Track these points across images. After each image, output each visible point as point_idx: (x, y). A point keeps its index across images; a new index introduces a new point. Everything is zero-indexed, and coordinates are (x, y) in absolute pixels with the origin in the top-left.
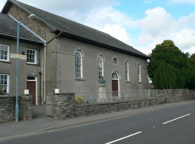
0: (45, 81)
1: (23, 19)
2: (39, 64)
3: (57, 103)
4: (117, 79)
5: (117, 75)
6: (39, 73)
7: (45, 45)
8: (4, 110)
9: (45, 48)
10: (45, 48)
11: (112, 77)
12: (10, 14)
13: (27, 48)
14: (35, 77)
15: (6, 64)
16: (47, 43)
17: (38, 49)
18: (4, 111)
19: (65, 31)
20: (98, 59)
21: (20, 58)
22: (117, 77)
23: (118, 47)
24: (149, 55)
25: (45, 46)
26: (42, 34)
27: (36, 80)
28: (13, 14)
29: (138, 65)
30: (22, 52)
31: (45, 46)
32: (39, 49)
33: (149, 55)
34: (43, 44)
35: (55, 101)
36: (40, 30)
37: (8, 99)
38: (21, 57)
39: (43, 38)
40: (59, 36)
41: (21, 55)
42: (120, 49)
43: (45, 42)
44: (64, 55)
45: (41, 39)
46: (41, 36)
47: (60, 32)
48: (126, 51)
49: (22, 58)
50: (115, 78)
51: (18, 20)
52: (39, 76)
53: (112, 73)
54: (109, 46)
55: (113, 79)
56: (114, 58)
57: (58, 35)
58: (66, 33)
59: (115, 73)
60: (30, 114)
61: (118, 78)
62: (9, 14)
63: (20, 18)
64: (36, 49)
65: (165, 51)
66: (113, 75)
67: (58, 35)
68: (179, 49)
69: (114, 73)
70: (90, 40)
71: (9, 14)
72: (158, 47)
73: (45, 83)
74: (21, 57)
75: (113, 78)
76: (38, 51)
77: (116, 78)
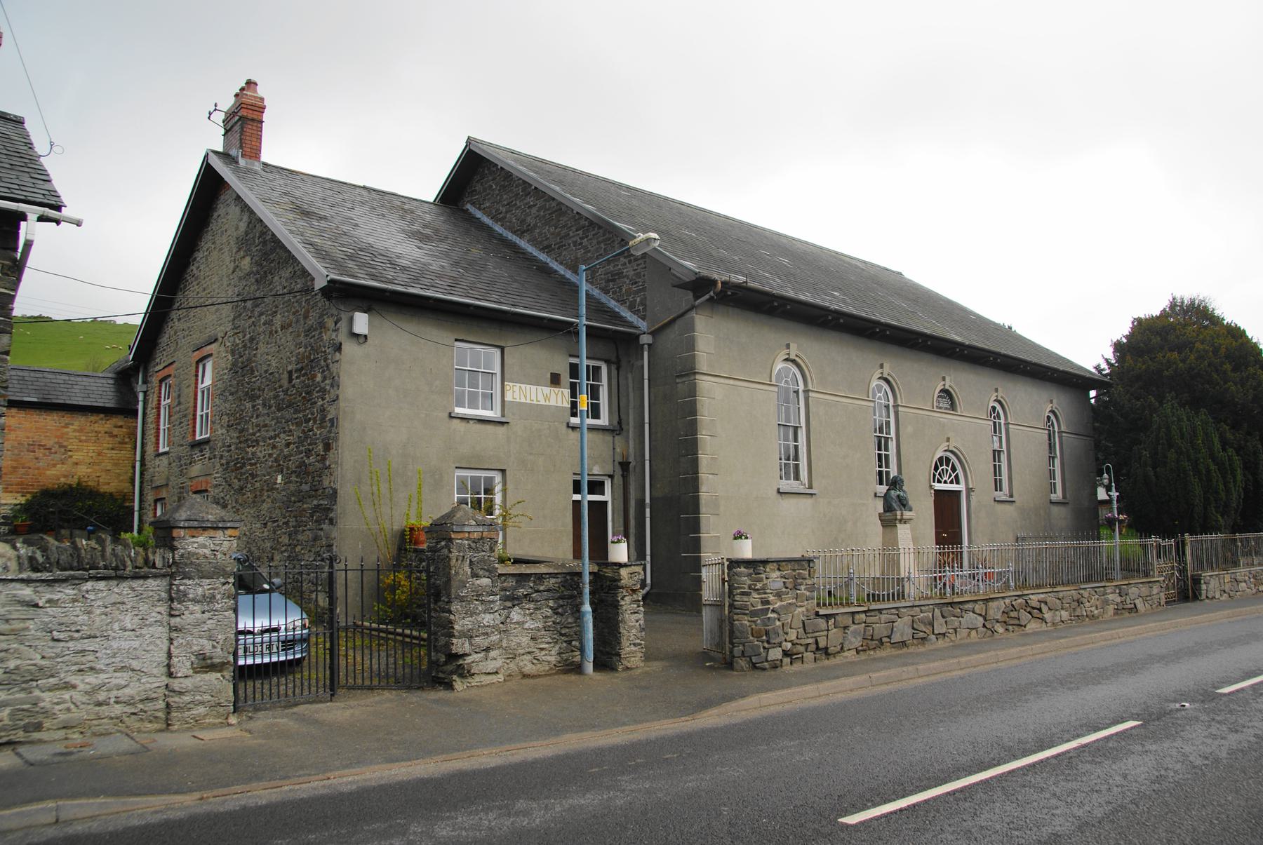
0: (648, 500)
1: (535, 226)
2: (620, 423)
3: (745, 598)
4: (954, 487)
5: (954, 469)
6: (620, 463)
7: (646, 339)
8: (536, 625)
9: (646, 354)
10: (646, 354)
11: (934, 475)
12: (473, 204)
13: (571, 356)
14: (602, 484)
15: (490, 428)
16: (653, 333)
17: (614, 359)
18: (539, 630)
19: (739, 279)
20: (874, 396)
21: (542, 402)
22: (957, 477)
23: (958, 339)
24: (1097, 368)
25: (646, 346)
26: (629, 292)
27: (607, 497)
28: (489, 208)
29: (1049, 418)
30: (549, 376)
31: (646, 346)
32: (618, 357)
33: (1097, 368)
34: (637, 337)
35: (738, 591)
36: (620, 274)
37: (553, 581)
38: (547, 398)
39: (631, 308)
40: (711, 299)
41: (547, 390)
42: (970, 347)
43: (643, 325)
44: (731, 382)
45: (623, 314)
46: (622, 302)
47: (714, 282)
48: (998, 355)
49: (553, 403)
50: (945, 482)
51: (514, 232)
52: (618, 479)
53: (939, 454)
54: (878, 323)
55: (938, 486)
56: (941, 391)
57: (707, 297)
58: (739, 287)
59: (948, 460)
60: (634, 645)
61: (958, 483)
62: (469, 206)
63: (523, 221)
64: (608, 362)
65: (1179, 348)
66: (936, 468)
67: (707, 297)
68: (1249, 334)
69: (941, 459)
70: (785, 300)
71: (469, 206)
72: (1141, 327)
73: (648, 511)
74: (547, 398)
75: (939, 482)
76: (613, 367)
77: (951, 482)
